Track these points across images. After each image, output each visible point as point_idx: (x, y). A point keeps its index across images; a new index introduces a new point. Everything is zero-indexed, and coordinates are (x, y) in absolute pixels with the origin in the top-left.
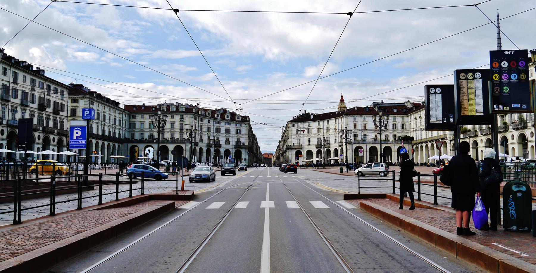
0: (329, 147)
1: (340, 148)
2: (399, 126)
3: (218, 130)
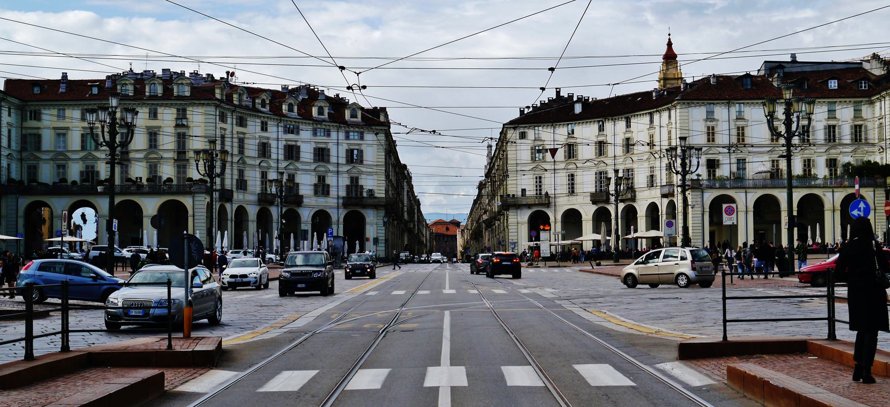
0: (633, 199)
1: (666, 201)
2: (845, 133)
3: (292, 152)
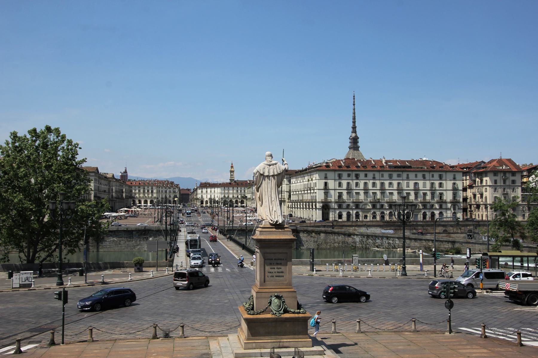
3: (166, 192)
